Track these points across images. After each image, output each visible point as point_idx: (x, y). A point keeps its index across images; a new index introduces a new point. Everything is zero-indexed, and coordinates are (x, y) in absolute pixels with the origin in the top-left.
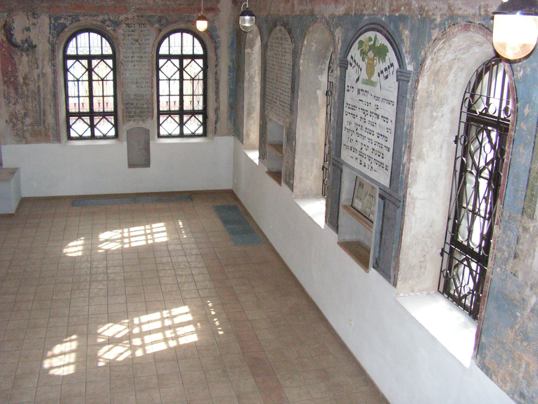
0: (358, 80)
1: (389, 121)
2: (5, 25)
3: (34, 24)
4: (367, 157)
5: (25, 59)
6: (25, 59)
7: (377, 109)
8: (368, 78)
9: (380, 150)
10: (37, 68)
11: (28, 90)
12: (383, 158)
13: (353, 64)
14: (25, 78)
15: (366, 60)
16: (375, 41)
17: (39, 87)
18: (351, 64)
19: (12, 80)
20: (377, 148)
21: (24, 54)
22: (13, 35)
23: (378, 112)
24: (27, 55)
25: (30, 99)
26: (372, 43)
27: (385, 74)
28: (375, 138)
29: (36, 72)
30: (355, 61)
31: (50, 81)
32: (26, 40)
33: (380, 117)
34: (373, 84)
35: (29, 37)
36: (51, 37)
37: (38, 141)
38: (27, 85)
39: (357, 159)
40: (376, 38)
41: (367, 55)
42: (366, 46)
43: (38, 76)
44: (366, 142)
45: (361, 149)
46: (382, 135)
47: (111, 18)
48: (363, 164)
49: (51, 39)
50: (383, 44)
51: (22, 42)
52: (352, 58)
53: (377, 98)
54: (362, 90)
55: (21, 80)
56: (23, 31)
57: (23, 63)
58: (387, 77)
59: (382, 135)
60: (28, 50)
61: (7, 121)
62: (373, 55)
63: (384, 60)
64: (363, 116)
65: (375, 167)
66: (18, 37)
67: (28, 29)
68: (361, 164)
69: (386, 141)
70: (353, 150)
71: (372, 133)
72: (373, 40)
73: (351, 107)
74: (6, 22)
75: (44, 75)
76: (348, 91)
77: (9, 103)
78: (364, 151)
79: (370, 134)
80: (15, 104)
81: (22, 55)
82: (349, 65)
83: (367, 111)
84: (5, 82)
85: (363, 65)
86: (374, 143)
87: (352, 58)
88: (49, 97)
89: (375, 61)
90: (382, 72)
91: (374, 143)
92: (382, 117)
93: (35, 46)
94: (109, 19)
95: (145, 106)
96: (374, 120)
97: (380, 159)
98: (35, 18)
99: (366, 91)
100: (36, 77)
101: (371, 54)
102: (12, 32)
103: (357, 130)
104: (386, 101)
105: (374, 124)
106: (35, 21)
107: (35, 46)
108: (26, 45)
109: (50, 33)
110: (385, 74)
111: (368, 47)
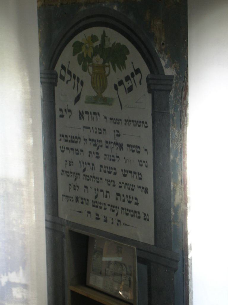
0: (77, 99)
1: (142, 150)
4: (108, 208)
7: (119, 136)
8: (95, 94)
9: (130, 193)
12: (137, 204)
13: (68, 77)
15: (90, 69)
16: (103, 41)
18: (63, 78)
20: (124, 191)
23: (119, 140)
26: (98, 43)
27: (127, 85)
28: (119, 178)
30: (69, 73)
33: (125, 146)
34: (106, 101)
39: (89, 212)
40: (104, 36)
41: (90, 61)
42: (87, 48)
44: (104, 186)
45: (96, 197)
46: (131, 172)
48: (102, 219)
50: (119, 44)
52: (63, 67)
53: (116, 121)
54: (87, 113)
58: (130, 89)
59: (131, 172)
62: (101, 61)
63: (122, 65)
64: (94, 149)
65: (123, 217)
68: (98, 219)
69: (140, 179)
70: (80, 200)
71: (113, 171)
72: (100, 39)
73: (69, 139)
76: (62, 116)
78: (101, 199)
79: (110, 173)
82: (59, 79)
83: (100, 141)
85: (86, 77)
86: (117, 185)
87: (63, 67)
89: (107, 69)
90: (121, 83)
91: (117, 185)
92: (128, 145)
96: (116, 151)
97: (132, 207)
99: (95, 114)
101: (98, 60)
103: (84, 170)
104: (132, 124)
105: (116, 158)
110: (127, 85)
111: (91, 51)
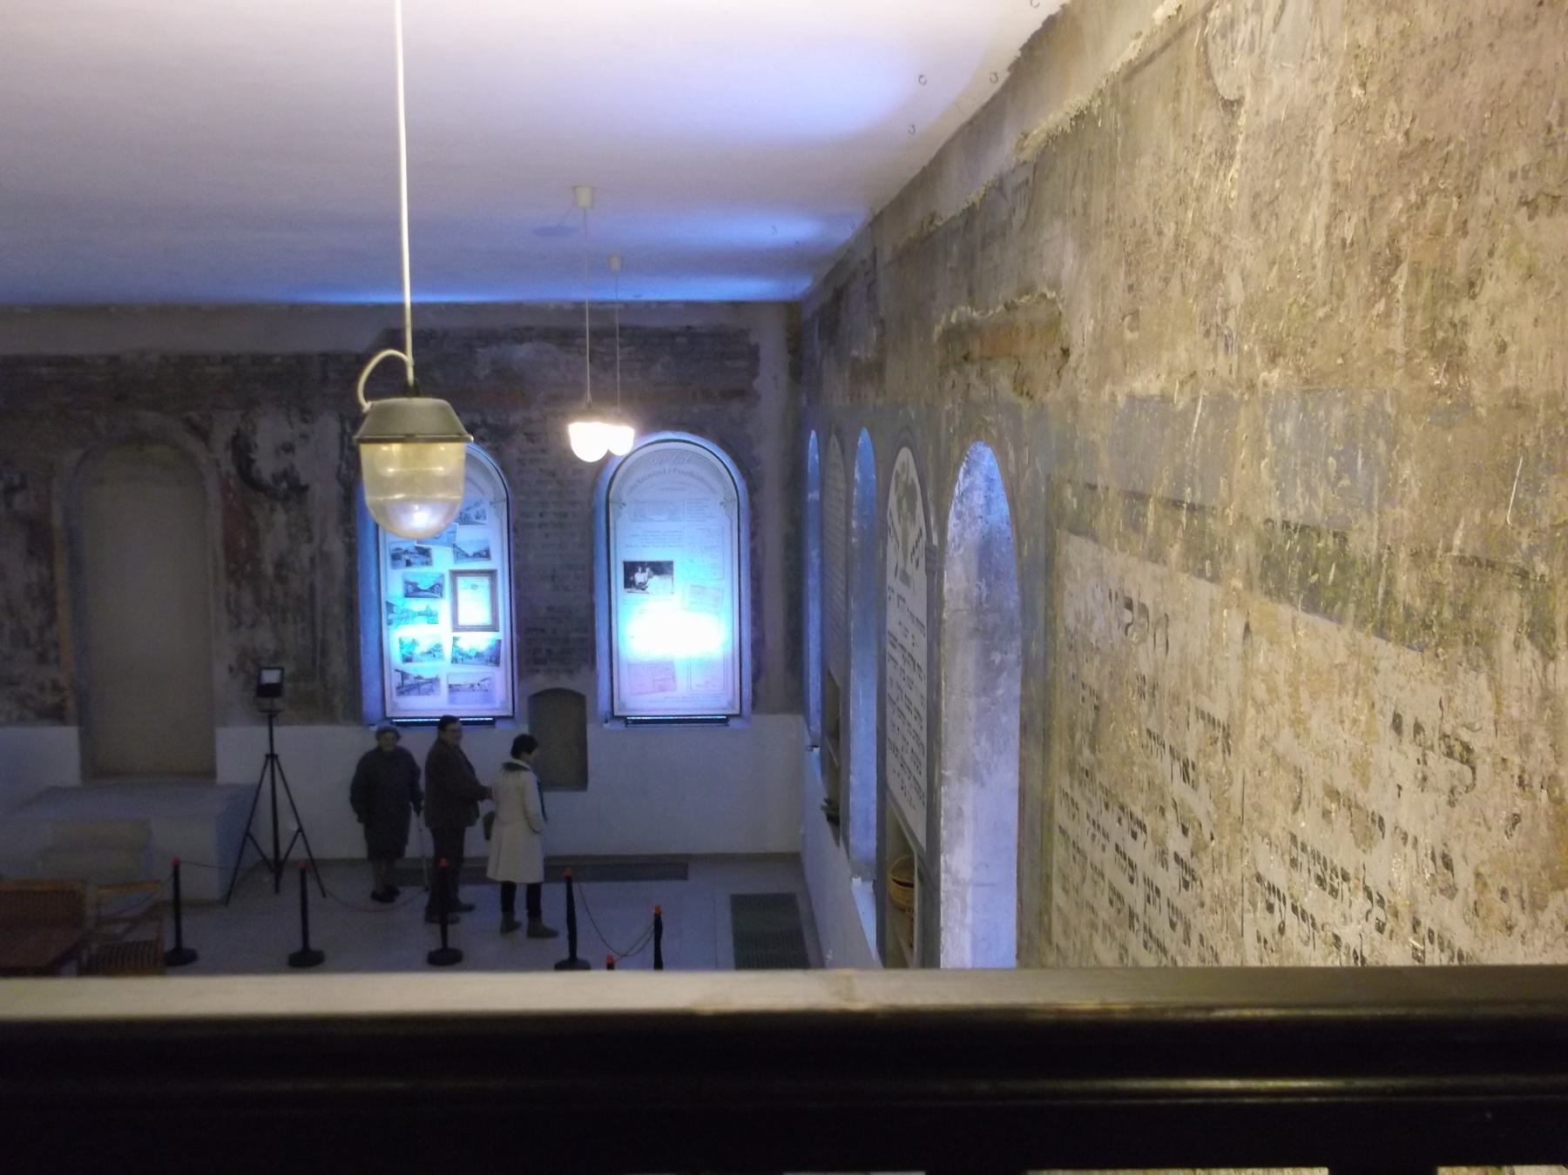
2: (235, 438)
3: (304, 436)
5: (280, 517)
6: (280, 517)
10: (310, 540)
11: (286, 594)
14: (280, 565)
17: (312, 587)
19: (249, 568)
21: (279, 506)
22: (253, 461)
24: (287, 511)
25: (289, 615)
29: (306, 551)
31: (340, 572)
32: (285, 475)
35: (292, 467)
36: (344, 466)
37: (310, 720)
38: (281, 579)
43: (312, 560)
47: (490, 420)
49: (344, 470)
51: (277, 478)
55: (269, 569)
56: (277, 452)
57: (276, 525)
60: (286, 498)
61: (231, 669)
66: (266, 465)
67: (289, 448)
74: (238, 430)
75: (326, 557)
77: (239, 624)
80: (253, 626)
81: (272, 510)
84: (231, 575)
88: (337, 610)
93: (306, 488)
94: (484, 423)
95: (574, 635)
98: (306, 421)
100: (306, 562)
102: (253, 456)
106: (304, 427)
107: (306, 488)
108: (284, 485)
109: (341, 458)
